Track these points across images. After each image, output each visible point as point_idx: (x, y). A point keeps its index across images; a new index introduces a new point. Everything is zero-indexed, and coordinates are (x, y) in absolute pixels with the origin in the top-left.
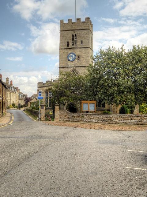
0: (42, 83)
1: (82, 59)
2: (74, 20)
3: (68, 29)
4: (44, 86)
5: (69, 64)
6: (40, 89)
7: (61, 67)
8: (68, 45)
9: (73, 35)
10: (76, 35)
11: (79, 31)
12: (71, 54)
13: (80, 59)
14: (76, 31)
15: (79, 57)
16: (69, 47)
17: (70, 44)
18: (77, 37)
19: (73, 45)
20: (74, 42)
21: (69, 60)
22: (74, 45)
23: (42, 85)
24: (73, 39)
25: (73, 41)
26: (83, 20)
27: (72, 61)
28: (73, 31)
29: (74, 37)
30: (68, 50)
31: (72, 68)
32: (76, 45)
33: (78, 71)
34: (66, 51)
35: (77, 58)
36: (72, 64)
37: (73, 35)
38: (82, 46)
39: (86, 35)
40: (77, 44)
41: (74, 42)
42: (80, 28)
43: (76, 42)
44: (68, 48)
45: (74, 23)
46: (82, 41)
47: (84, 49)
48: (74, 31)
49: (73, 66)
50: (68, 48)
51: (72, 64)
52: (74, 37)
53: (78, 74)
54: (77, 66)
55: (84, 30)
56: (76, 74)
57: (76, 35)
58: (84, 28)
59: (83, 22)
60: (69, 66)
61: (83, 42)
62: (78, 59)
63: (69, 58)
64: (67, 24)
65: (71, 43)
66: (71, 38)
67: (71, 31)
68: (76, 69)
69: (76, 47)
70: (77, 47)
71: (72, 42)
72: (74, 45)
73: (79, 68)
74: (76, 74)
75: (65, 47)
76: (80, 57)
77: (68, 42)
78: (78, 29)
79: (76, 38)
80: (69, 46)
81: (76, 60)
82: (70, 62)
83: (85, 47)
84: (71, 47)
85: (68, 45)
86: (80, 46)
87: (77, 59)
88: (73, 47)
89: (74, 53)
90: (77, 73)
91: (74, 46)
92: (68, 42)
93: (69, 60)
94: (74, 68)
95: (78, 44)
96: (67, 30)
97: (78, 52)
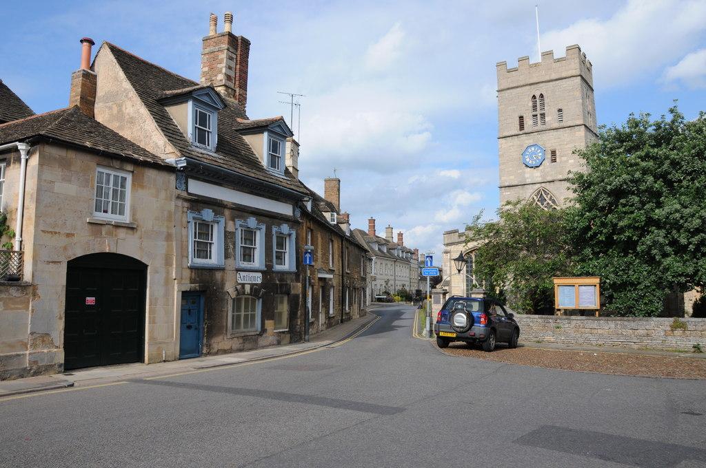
0: (455, 231)
1: (564, 159)
2: (537, 58)
3: (519, 84)
4: (460, 240)
5: (527, 176)
6: (449, 248)
7: (507, 184)
8: (522, 126)
9: (534, 97)
10: (542, 96)
11: (551, 83)
12: (533, 149)
13: (558, 160)
14: (541, 85)
15: (554, 153)
16: (526, 129)
17: (529, 122)
18: (546, 100)
19: (535, 123)
20: (539, 116)
21: (527, 166)
22: (539, 122)
23: (455, 238)
24: (535, 107)
25: (535, 113)
26: (560, 53)
28: (532, 86)
29: (538, 101)
31: (538, 186)
32: (544, 123)
33: (554, 192)
34: (516, 140)
35: (549, 156)
36: (536, 175)
37: (534, 97)
40: (547, 119)
41: (539, 116)
42: (554, 76)
43: (543, 115)
44: (521, 132)
45: (536, 65)
46: (560, 110)
49: (540, 180)
50: (521, 132)
51: (536, 175)
52: (538, 101)
53: (554, 202)
54: (549, 179)
55: (565, 78)
56: (550, 202)
57: (542, 96)
58: (564, 75)
59: (559, 60)
60: (529, 181)
61: (564, 112)
62: (554, 161)
63: (528, 160)
64: (516, 70)
65: (531, 117)
66: (531, 104)
67: (528, 87)
68: (548, 186)
69: (544, 127)
70: (549, 128)
71: (534, 116)
72: (539, 122)
73: (557, 183)
74: (550, 202)
75: (516, 130)
76: (557, 152)
77: (521, 118)
78: (547, 78)
79: (543, 104)
80: (525, 126)
81: (547, 163)
82: (529, 169)
83: (572, 124)
84: (530, 130)
85: (522, 126)
86: (556, 125)
87: (550, 160)
88: (536, 128)
89: (540, 144)
90: (550, 199)
91: (540, 127)
92: (521, 118)
93: (527, 166)
94: (543, 185)
96: (517, 87)
97: (550, 140)
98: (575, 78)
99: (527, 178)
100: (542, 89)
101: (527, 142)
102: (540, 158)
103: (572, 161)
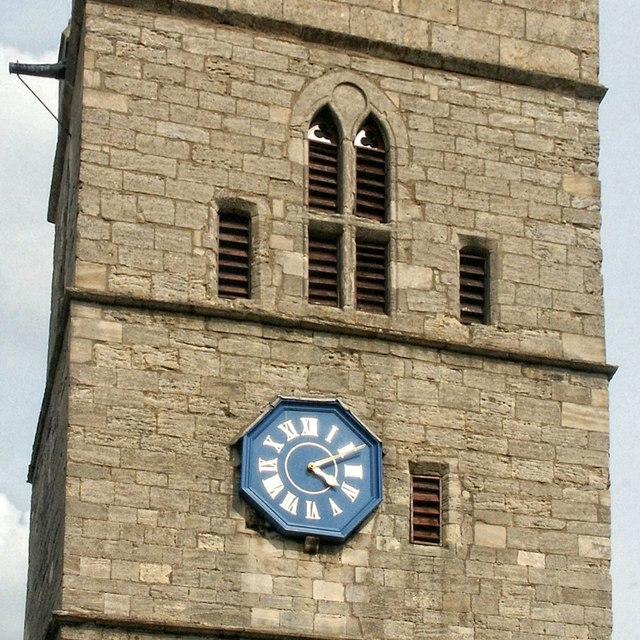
1: (491, 535)
8: (237, 265)
10: (373, 126)
13: (454, 533)
14: (374, 65)
15: (429, 485)
18: (402, 170)
25: (323, 217)
27: (326, 545)
28: (322, 54)
30: (252, 343)
32: (376, 295)
37: (326, 119)
38: (483, 335)
39: (549, 178)
40: (403, 276)
47: (523, 382)
48: (343, 58)
69: (375, 320)
70: (412, 329)
77: (235, 218)
81: (389, 533)
85: (237, 265)
86: (454, 330)
87: (404, 525)
92: (235, 218)
95: (421, 282)
98: (569, 101)
99: (263, 600)
100: (390, 92)
101: (273, 375)
102: (352, 493)
103: (538, 560)
